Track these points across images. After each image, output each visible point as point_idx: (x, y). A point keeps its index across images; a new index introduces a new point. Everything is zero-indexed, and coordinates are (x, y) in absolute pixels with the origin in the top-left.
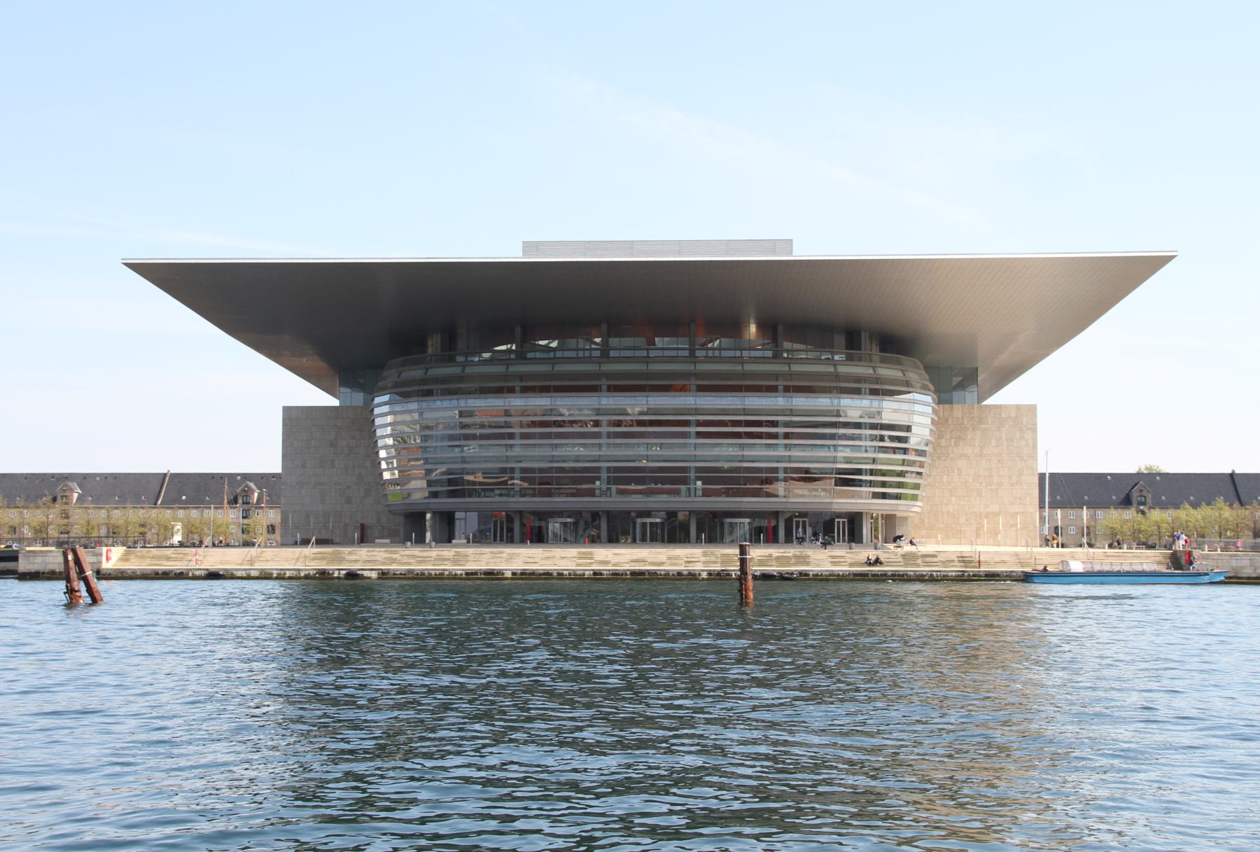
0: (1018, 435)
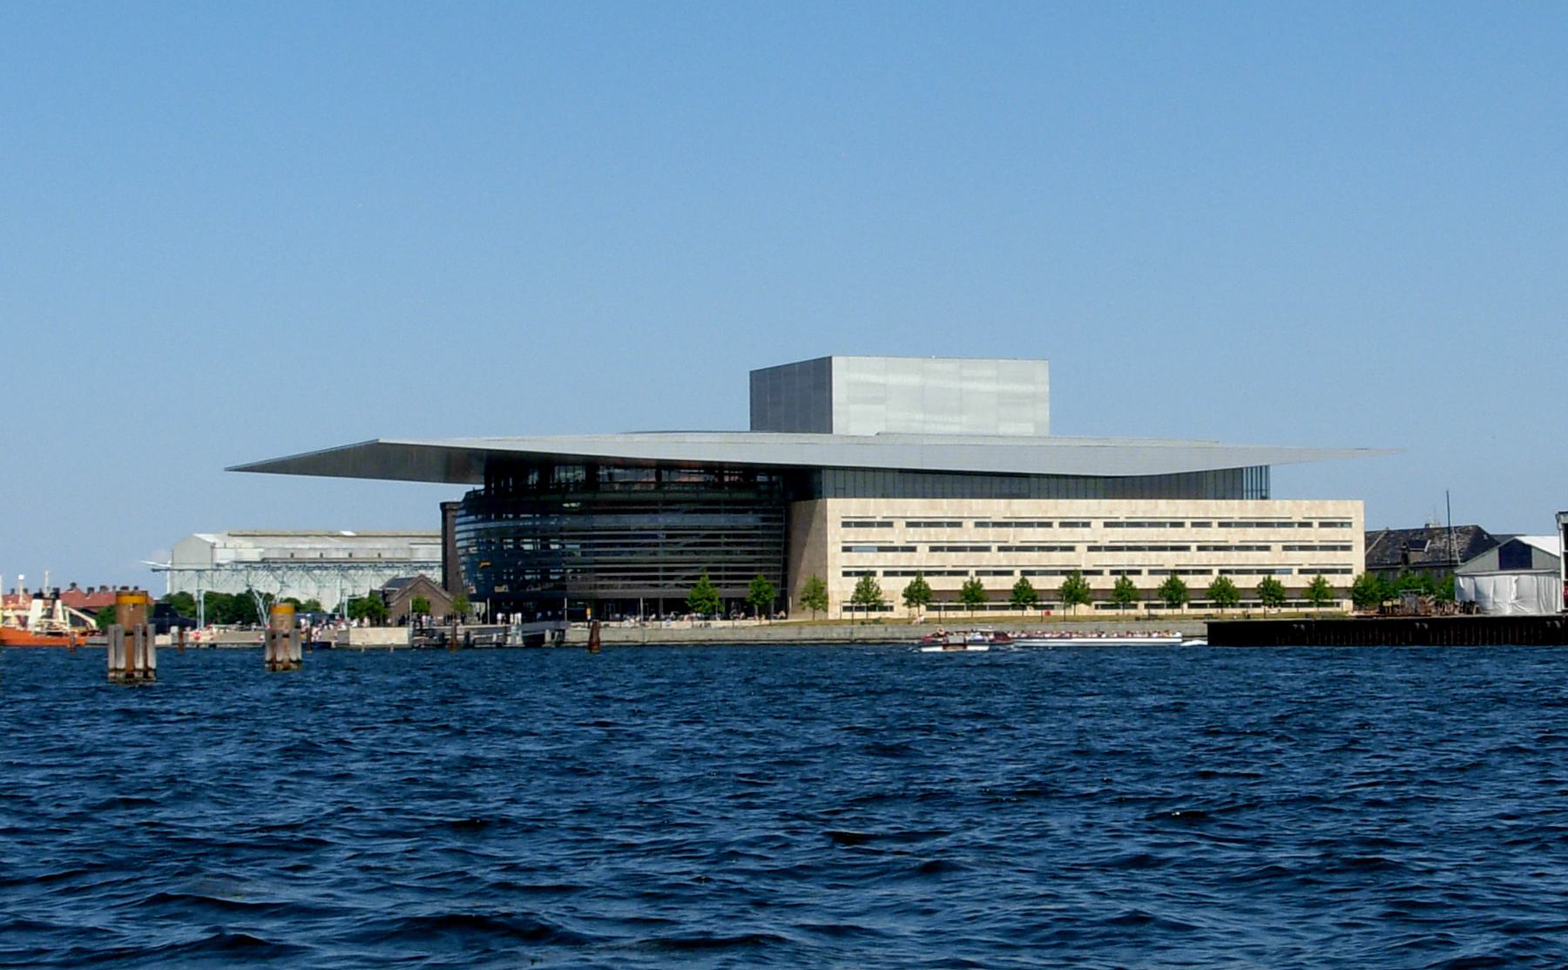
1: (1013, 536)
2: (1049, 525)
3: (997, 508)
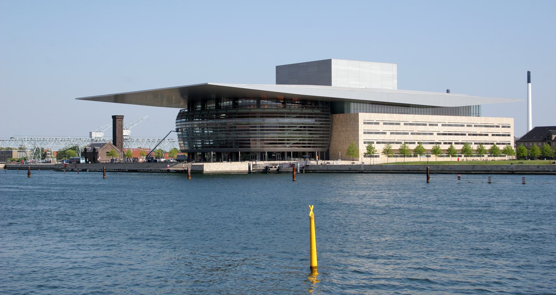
0: (355, 124)
2: (425, 125)
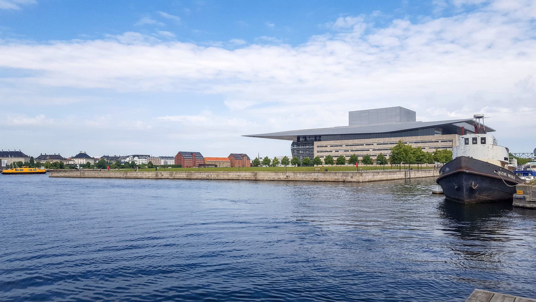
1: (354, 148)
2: (363, 145)
3: (350, 142)
